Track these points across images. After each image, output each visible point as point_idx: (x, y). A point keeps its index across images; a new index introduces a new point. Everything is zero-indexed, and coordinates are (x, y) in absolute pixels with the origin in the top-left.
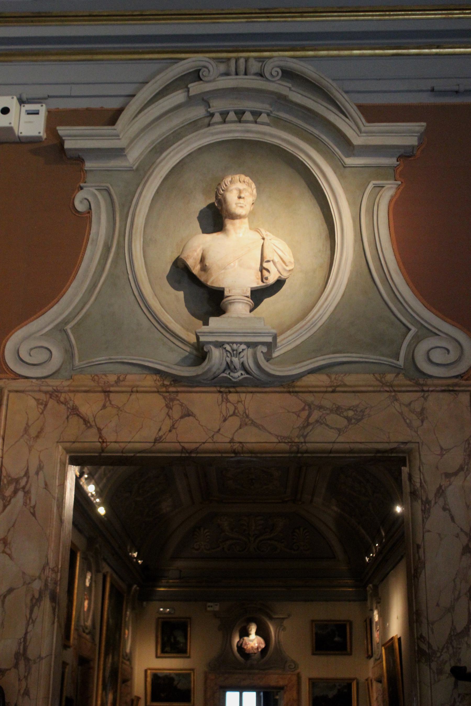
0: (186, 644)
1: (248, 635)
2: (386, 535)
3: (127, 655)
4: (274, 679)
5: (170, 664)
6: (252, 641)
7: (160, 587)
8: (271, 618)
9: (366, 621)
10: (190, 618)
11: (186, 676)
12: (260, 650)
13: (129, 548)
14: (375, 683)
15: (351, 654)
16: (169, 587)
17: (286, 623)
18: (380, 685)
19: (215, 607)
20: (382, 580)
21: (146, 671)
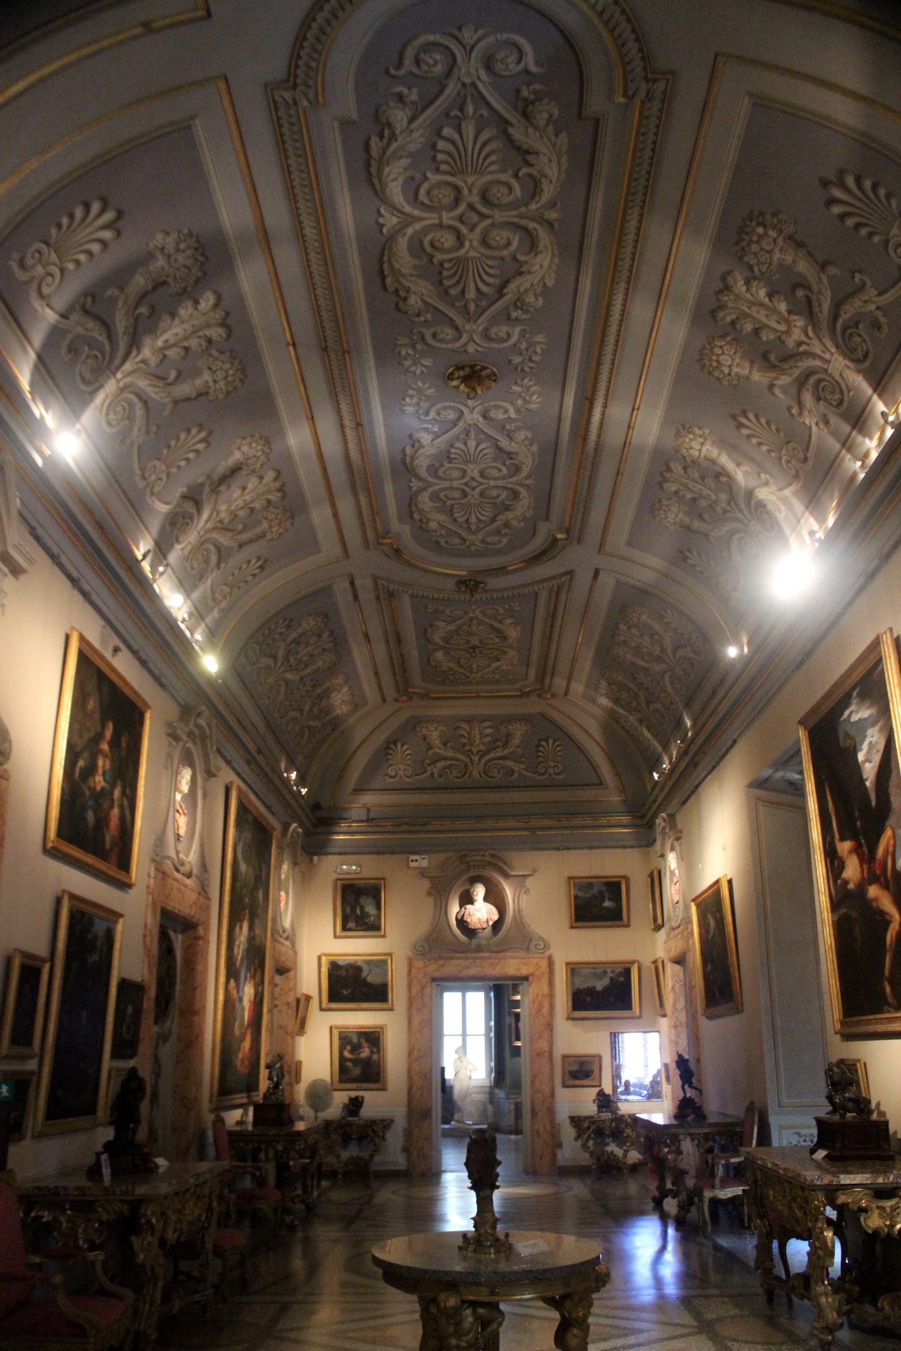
0: (379, 916)
1: (471, 902)
3: (284, 931)
4: (512, 966)
5: (357, 947)
6: (479, 910)
7: (338, 833)
8: (506, 876)
9: (651, 875)
10: (384, 879)
11: (380, 964)
12: (491, 923)
13: (283, 766)
14: (669, 966)
16: (353, 833)
17: (529, 882)
18: (677, 967)
19: (423, 862)
21: (319, 958)
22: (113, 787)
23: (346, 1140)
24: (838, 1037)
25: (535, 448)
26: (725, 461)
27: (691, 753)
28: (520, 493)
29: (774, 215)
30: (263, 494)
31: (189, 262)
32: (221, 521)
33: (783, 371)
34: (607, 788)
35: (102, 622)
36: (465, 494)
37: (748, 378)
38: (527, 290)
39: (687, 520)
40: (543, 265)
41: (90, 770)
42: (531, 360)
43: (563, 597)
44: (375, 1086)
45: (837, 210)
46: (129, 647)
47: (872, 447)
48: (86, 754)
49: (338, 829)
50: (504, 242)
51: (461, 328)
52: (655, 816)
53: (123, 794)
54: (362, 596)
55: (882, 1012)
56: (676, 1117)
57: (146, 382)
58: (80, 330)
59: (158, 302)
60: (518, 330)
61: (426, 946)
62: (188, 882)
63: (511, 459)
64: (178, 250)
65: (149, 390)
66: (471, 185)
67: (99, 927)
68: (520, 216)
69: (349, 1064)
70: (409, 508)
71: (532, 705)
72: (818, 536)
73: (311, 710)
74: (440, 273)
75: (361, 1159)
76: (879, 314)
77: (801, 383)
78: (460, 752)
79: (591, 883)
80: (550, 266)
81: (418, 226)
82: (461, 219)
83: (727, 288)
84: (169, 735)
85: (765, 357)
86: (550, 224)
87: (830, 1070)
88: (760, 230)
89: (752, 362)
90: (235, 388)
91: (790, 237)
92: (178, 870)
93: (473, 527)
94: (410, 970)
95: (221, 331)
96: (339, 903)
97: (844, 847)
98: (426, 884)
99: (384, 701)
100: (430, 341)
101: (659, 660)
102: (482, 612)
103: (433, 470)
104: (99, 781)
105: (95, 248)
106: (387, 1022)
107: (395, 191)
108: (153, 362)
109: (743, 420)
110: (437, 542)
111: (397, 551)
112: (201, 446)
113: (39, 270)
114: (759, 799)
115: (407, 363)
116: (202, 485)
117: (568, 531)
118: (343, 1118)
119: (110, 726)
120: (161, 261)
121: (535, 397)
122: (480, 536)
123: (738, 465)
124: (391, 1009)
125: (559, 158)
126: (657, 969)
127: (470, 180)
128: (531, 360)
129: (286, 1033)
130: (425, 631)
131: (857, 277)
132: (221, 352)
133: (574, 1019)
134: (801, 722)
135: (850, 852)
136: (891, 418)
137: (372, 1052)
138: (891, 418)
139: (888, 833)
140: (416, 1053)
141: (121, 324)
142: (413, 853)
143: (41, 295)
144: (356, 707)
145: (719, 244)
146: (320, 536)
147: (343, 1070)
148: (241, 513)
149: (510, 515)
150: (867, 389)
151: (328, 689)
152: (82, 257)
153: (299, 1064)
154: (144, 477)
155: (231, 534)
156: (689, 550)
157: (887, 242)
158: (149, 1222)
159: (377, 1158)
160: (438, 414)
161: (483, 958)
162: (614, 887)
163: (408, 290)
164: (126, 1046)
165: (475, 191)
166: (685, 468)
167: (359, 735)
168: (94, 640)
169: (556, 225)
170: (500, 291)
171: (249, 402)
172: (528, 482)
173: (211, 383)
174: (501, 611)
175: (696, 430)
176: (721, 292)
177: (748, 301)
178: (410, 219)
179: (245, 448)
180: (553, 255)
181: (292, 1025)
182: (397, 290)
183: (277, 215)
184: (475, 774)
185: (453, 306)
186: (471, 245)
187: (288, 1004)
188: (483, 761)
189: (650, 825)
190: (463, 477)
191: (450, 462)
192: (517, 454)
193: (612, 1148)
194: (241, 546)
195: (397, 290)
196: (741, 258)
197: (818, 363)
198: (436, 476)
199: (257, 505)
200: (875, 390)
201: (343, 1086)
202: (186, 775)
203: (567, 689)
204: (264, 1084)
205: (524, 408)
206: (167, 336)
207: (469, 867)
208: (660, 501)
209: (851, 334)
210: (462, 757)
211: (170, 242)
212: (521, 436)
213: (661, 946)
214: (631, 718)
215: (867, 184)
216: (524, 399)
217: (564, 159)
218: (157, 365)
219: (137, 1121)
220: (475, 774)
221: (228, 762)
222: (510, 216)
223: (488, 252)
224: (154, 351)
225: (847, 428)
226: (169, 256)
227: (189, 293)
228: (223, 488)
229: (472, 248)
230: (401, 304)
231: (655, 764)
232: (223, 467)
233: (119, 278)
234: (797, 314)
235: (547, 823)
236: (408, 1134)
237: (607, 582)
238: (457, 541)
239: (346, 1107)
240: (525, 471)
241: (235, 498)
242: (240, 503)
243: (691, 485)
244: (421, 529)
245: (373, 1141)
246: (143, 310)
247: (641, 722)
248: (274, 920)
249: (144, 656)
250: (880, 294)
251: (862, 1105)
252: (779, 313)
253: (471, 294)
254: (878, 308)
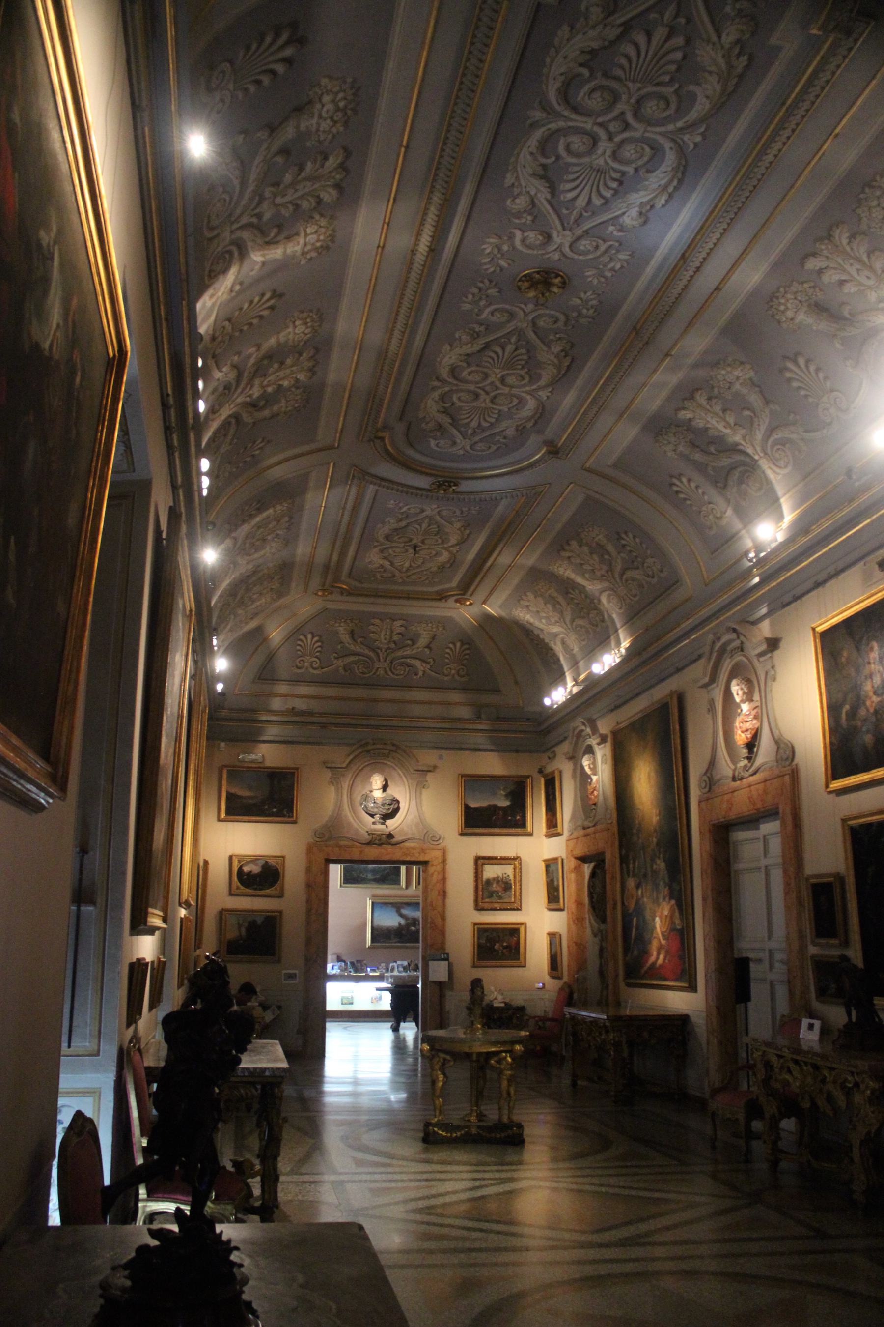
25: (509, 180)
26: (277, 253)
28: (559, 91)
38: (467, 344)
40: (449, 357)
42: (480, 289)
51: (531, 325)
60: (483, 317)
63: (544, 166)
64: (670, 443)
65: (763, 428)
68: (457, 385)
80: (444, 356)
81: (528, 388)
86: (438, 379)
95: (698, 396)
100: (562, 318)
105: (693, 485)
108: (743, 431)
115: (594, 302)
120: (681, 448)
121: (488, 251)
123: (264, 263)
128: (480, 289)
132: (713, 387)
163: (557, 356)
166: (319, 201)
170: (487, 346)
175: (314, 254)
176: (314, 366)
180: (440, 363)
185: (528, 342)
191: (624, 174)
192: (534, 175)
206: (720, 427)
208: (346, 124)
212: (521, 202)
216: (499, 250)
218: (744, 428)
222: (463, 386)
227: (688, 426)
253: (510, 348)
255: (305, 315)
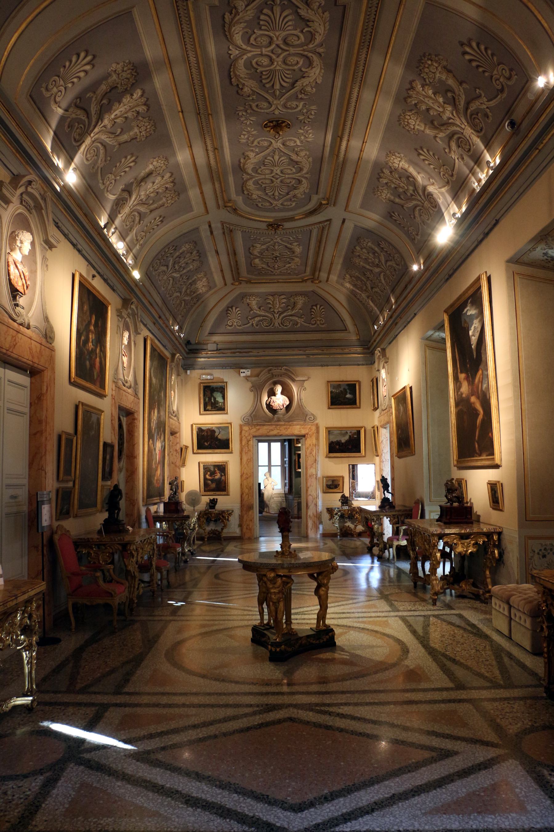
0: (224, 403)
1: (274, 395)
2: (396, 302)
4: (296, 429)
5: (212, 420)
8: (293, 380)
9: (372, 380)
11: (226, 428)
15: (359, 408)
16: (208, 357)
17: (306, 384)
19: (248, 372)
20: (390, 343)
21: (192, 426)
22: (96, 347)
23: (208, 521)
24: (456, 468)
27: (394, 318)
29: (436, 56)
30: (164, 184)
31: (129, 76)
32: (141, 200)
33: (441, 131)
34: (349, 332)
35: (87, 263)
36: (272, 182)
37: (423, 132)
39: (392, 198)
40: (316, 73)
41: (86, 341)
42: (309, 118)
43: (326, 232)
44: (224, 493)
45: (467, 57)
46: (99, 273)
47: (483, 176)
48: (84, 333)
49: (200, 355)
50: (295, 62)
52: (375, 349)
53: (101, 350)
54: (215, 233)
55: (473, 457)
56: (380, 507)
57: (106, 136)
58: (74, 116)
59: (113, 96)
60: (302, 104)
61: (249, 418)
62: (129, 391)
64: (123, 71)
65: (107, 140)
66: (278, 36)
67: (94, 418)
68: (304, 50)
69: (210, 482)
70: (242, 189)
71: (309, 287)
72: (457, 216)
73: (186, 291)
74: (261, 77)
75: (217, 530)
76: (488, 110)
77: (450, 137)
78: (267, 312)
79: (340, 385)
81: (249, 55)
82: (272, 51)
83: (412, 88)
84: (118, 316)
85: (432, 122)
86: (320, 54)
87: (447, 483)
88: (429, 62)
89: (425, 125)
90: (151, 134)
91: (445, 67)
92: (124, 385)
93: (277, 198)
94: (241, 433)
95: (145, 108)
96: (202, 396)
97: (462, 376)
98: (249, 385)
99: (226, 285)
101: (378, 266)
102: (281, 240)
103: (255, 170)
104: (90, 345)
105: (82, 74)
106: (230, 459)
107: (238, 39)
108: (109, 126)
109: (421, 152)
110: (257, 205)
111: (235, 210)
112: (132, 164)
113: (55, 90)
114: (426, 346)
115: (242, 119)
116: (132, 183)
117: (328, 199)
118: (206, 510)
119: (94, 317)
120: (114, 77)
122: (280, 201)
123: (419, 173)
124: (231, 453)
125: (324, 24)
126: (374, 431)
127: (277, 34)
128: (309, 118)
129: (176, 466)
130: (249, 249)
131: (478, 91)
133: (330, 457)
134: (445, 311)
135: (464, 379)
136: (492, 165)
137: (221, 476)
138: (492, 165)
139: (480, 372)
140: (244, 476)
141: (93, 109)
142: (242, 368)
143: (56, 102)
144: (210, 288)
145: (408, 67)
146: (193, 203)
147: (206, 484)
148: (152, 195)
149: (296, 192)
150: (482, 147)
151: (195, 280)
152: (75, 80)
153: (182, 482)
154: (103, 184)
155: (146, 206)
156: (393, 213)
157: (492, 77)
158: (131, 552)
159: (225, 531)
160: (259, 143)
161: (281, 425)
162: (352, 387)
163: (244, 85)
164: (108, 475)
165: (280, 39)
166: (391, 172)
167: (212, 302)
168: (84, 274)
169: (323, 55)
170: (293, 85)
171: (158, 140)
172: (306, 176)
173: (138, 133)
174: (291, 239)
175: (397, 154)
176: (409, 89)
177: (423, 95)
178: (245, 52)
179: (155, 163)
180: (321, 68)
181: (179, 463)
182: (238, 85)
183: (175, 49)
184: (276, 325)
186: (277, 64)
187: (176, 450)
188: (281, 317)
189: (372, 353)
190: (272, 173)
193: (349, 524)
194: (151, 211)
195: (238, 85)
196: (420, 75)
197: (458, 129)
198: (256, 172)
199: (160, 191)
200: (486, 147)
201: (206, 493)
202: (126, 335)
203: (328, 278)
204: (167, 492)
205: (304, 140)
206: (117, 112)
207: (273, 376)
209: (475, 118)
210: (269, 315)
211: (119, 67)
212: (302, 154)
213: (376, 418)
214: (363, 295)
215: (482, 48)
217: (327, 24)
219: (119, 510)
220: (276, 325)
221: (145, 325)
222: (299, 50)
223: (287, 67)
224: (110, 120)
225: (472, 163)
226: (118, 74)
227: (129, 91)
228: (143, 184)
229: (278, 65)
230: (240, 91)
231: (375, 320)
232: (143, 174)
233: (93, 87)
234: (448, 104)
235: (316, 351)
236: (241, 517)
237: (349, 227)
238: (268, 204)
239: (207, 504)
240: (305, 171)
241: (149, 188)
242: (152, 190)
243: (394, 180)
244: (248, 198)
245: (223, 521)
246: (104, 101)
247: (368, 297)
248: (169, 406)
249: (105, 277)
250: (488, 101)
251: (460, 499)
252: (439, 103)
253: (277, 86)
254: (487, 108)
255: (407, 128)
